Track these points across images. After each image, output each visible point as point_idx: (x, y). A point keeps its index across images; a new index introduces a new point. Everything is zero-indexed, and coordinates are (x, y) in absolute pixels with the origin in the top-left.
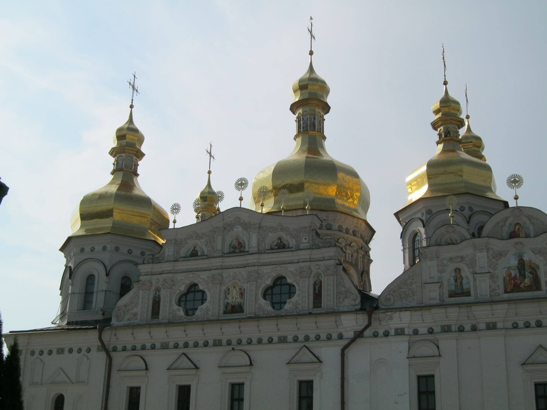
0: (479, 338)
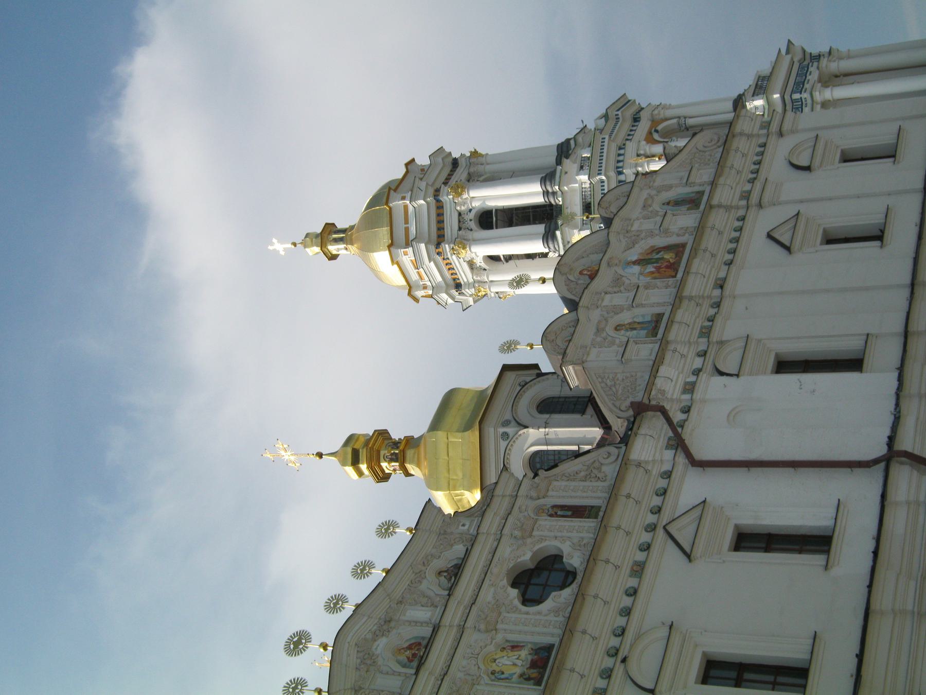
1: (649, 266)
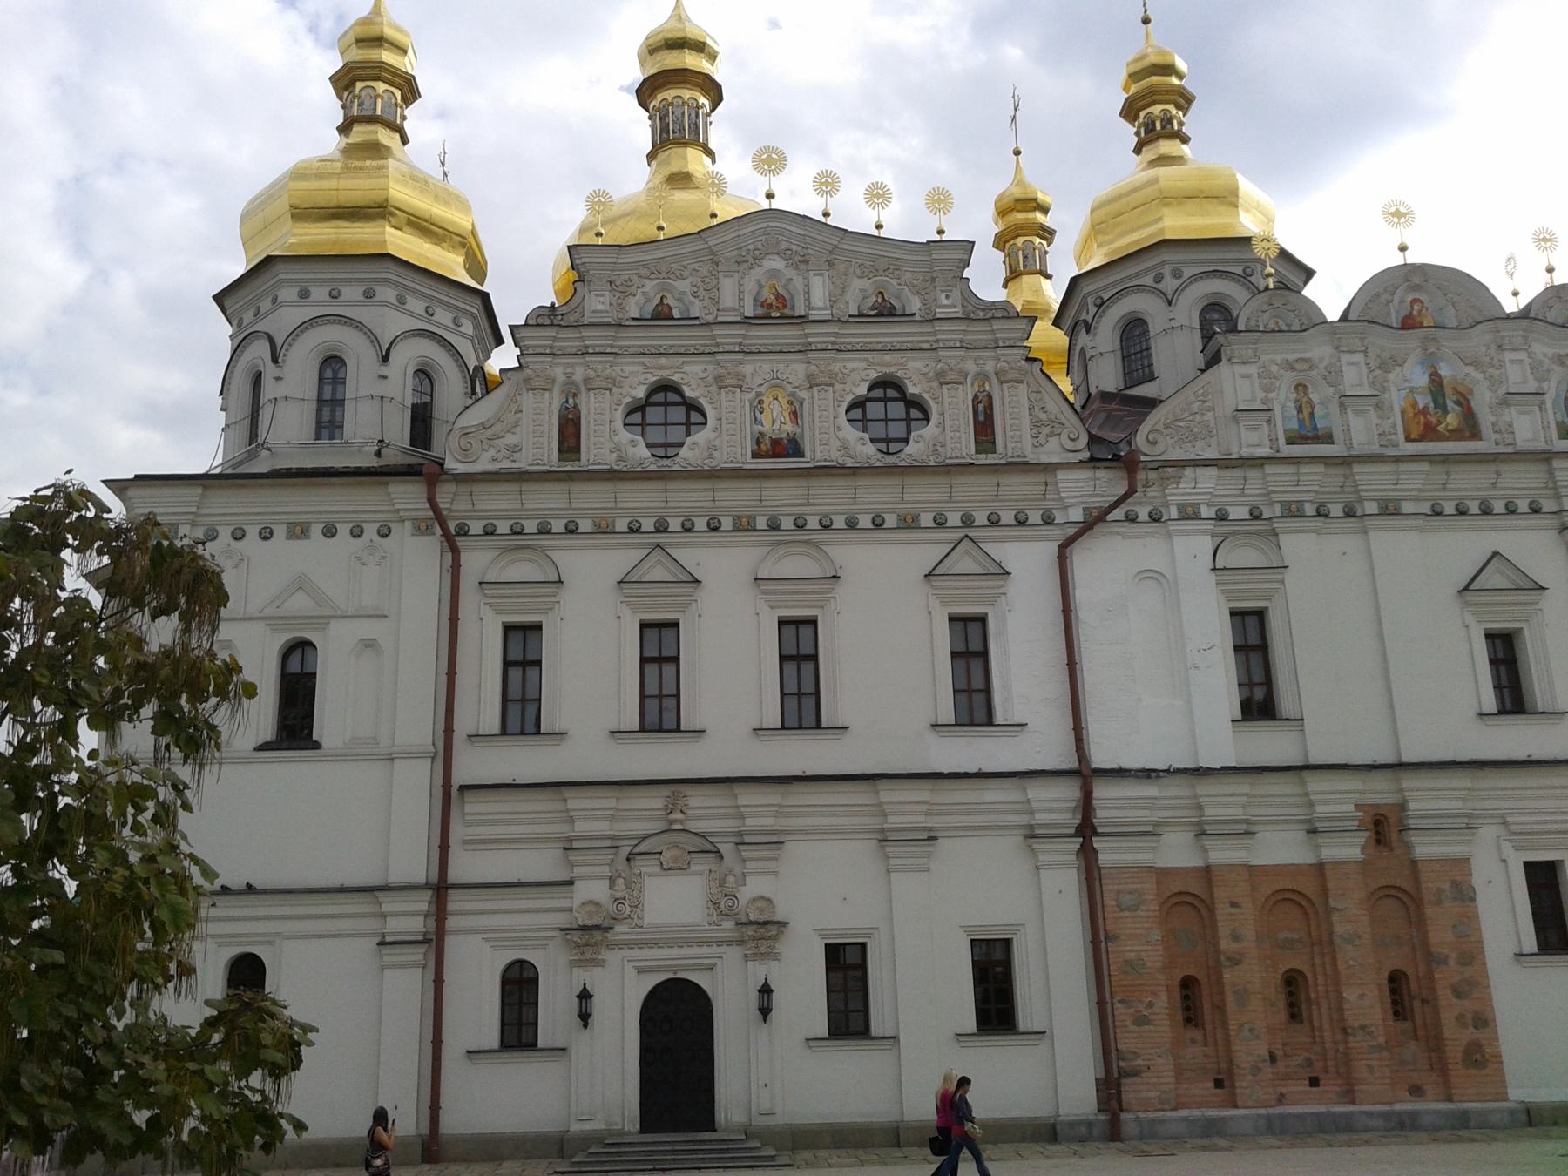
0: (1366, 533)
1: (1429, 398)
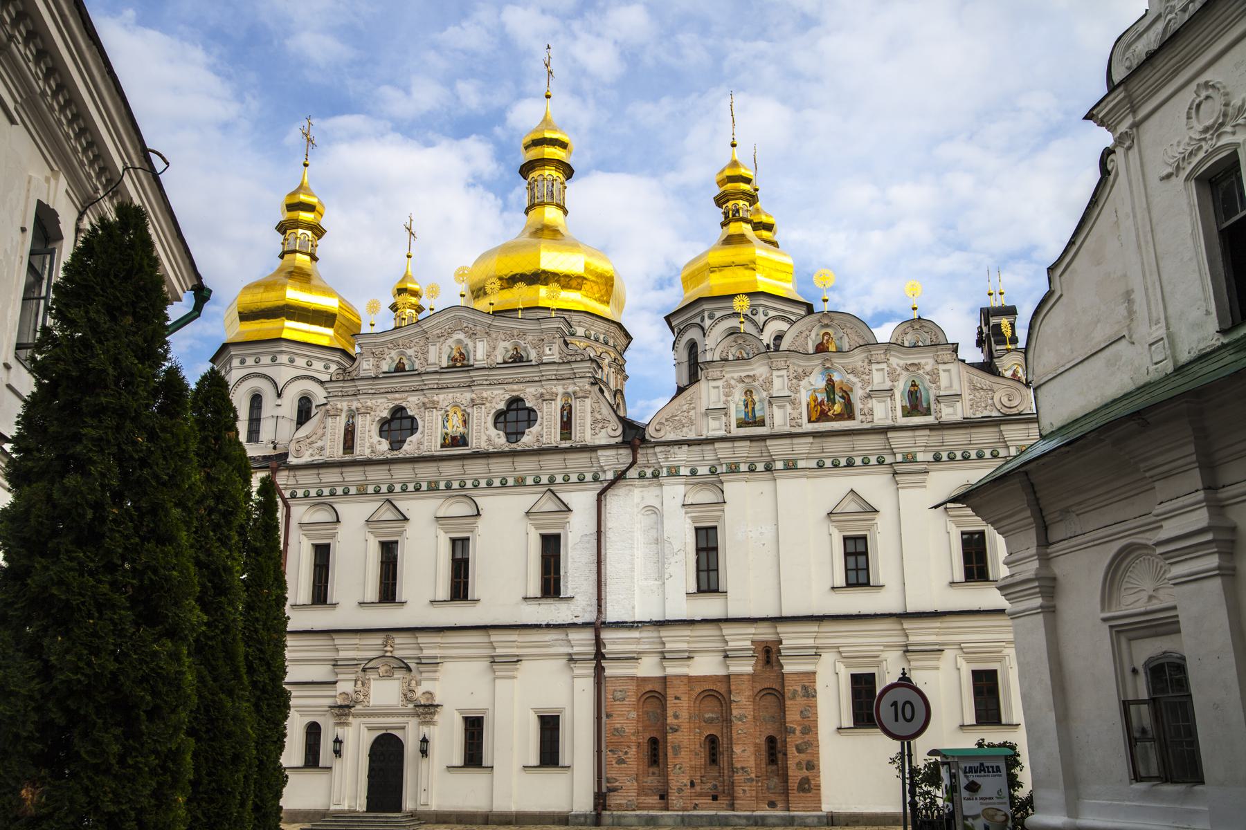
1: (825, 395)
